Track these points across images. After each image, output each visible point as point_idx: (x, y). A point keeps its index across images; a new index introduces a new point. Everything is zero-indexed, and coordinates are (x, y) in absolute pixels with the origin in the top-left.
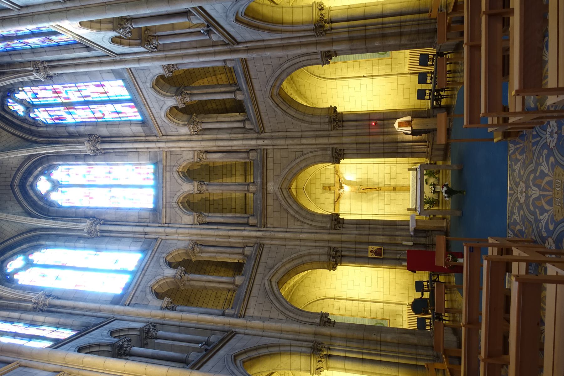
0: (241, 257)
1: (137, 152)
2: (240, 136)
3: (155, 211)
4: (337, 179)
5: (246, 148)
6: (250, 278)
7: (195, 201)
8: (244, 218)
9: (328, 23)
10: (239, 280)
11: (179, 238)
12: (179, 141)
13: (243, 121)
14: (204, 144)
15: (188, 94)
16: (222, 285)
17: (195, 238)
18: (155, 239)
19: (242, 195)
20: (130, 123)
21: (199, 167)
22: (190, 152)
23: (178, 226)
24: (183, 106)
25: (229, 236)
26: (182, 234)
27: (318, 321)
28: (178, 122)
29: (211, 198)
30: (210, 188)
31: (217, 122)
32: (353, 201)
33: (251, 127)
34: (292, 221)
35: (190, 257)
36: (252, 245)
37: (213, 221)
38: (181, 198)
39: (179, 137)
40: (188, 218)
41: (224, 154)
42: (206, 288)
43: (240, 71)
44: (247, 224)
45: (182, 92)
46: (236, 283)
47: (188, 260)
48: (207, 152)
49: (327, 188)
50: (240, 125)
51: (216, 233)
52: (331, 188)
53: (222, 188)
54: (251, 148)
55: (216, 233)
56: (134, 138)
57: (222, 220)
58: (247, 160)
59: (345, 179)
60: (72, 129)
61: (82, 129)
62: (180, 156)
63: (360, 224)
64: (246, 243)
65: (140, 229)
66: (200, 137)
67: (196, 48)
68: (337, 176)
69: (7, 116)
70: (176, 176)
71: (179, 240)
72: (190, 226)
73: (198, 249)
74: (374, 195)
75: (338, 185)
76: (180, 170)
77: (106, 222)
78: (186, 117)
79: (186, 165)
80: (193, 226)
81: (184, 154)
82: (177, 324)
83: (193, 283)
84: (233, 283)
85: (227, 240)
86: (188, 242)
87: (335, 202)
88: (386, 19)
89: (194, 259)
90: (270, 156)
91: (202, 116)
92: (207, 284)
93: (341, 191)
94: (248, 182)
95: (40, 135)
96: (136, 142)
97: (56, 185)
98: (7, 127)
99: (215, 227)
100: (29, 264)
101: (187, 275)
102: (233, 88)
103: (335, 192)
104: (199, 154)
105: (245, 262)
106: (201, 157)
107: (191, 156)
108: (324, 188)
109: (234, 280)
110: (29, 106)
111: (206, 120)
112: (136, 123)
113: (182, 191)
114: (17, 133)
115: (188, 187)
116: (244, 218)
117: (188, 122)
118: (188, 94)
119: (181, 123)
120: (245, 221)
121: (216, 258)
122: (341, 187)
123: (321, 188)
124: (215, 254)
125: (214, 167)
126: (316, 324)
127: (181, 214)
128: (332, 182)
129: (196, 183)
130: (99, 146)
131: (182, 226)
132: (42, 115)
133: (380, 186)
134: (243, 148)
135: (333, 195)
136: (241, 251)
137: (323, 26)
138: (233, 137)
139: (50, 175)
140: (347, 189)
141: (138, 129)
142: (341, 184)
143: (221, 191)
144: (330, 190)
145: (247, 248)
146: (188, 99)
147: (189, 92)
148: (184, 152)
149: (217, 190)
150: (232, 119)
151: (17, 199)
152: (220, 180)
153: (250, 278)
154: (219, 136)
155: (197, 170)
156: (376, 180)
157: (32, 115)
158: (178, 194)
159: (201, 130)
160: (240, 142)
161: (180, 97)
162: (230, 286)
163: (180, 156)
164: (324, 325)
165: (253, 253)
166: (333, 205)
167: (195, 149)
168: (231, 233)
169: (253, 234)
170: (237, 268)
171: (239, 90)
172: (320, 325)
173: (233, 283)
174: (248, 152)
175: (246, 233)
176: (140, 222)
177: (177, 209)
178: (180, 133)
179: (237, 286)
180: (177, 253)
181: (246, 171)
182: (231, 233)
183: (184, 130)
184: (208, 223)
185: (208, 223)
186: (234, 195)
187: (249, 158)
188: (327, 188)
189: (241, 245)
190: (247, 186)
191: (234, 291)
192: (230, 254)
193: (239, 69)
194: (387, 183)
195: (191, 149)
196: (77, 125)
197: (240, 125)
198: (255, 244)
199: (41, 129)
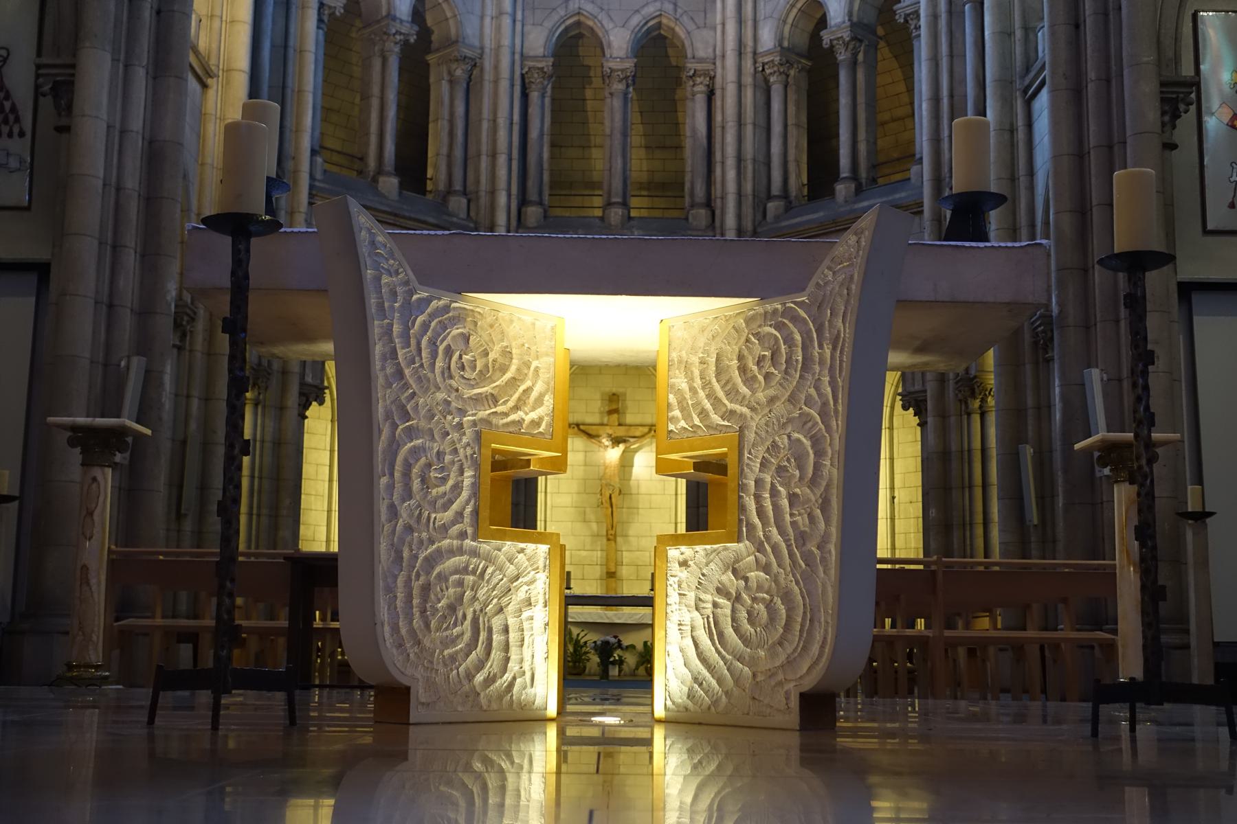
0: (442, 187)
2: (748, 187)
4: (638, 432)
5: (719, 202)
6: (396, 215)
7: (581, 51)
8: (540, 193)
9: (981, 407)
10: (389, 184)
11: (487, 20)
12: (740, 22)
13: (785, 195)
14: (731, 89)
15: (855, 55)
16: (373, 139)
17: (488, 64)
19: (596, 177)
21: (674, 62)
22: (710, 50)
23: (519, 16)
24: (826, 43)
25: (493, 156)
26: (499, 29)
27: (309, 379)
28: (790, 20)
29: (589, 93)
30: (617, 103)
31: (786, 126)
33: (770, 215)
35: (438, 50)
36: (472, 214)
37: (530, 110)
38: (590, 23)
39: (750, 23)
40: (538, 41)
41: (705, 141)
42: (366, 97)
43: (897, 196)
44: (523, 202)
45: (861, 41)
46: (382, 179)
47: (431, 42)
48: (710, 94)
50: (776, 187)
51: (502, 121)
52: (615, 416)
53: (618, 136)
54: (718, 212)
55: (502, 121)
57: (534, 134)
58: (687, 200)
59: (636, 451)
62: (701, 22)
64: (478, 198)
66: (748, 79)
67: (951, 96)
68: (646, 430)
70: (651, 9)
71: (482, 18)
72: (518, 48)
74: (594, 526)
75: (621, 432)
76: (664, 21)
78: (802, 41)
79: (679, 37)
80: (517, 57)
81: (706, 33)
82: (291, 43)
83: (377, 64)
84: (380, 171)
85: (484, 148)
86: (477, 43)
87: (578, 425)
88: (979, 531)
89: (431, 58)
91: (804, 85)
92: (375, 102)
93: (606, 442)
94: (634, 202)
99: (516, 118)
101: (397, 49)
102: (863, 173)
103: (602, 425)
104: (706, 74)
105: (429, 197)
106: (699, 80)
107: (701, 53)
109: (388, 174)
111: (792, 97)
113: (609, 25)
116: (540, 193)
117: (788, 49)
118: (855, 55)
119: (787, 28)
120: (533, 195)
121: (437, 120)
122: (616, 441)
123: (614, 390)
124: (446, 116)
125: (674, 101)
126: (303, 375)
127: (548, 24)
128: (629, 419)
129: (629, 64)
131: (519, 26)
133: (619, 539)
134: (719, 193)
135: (595, 419)
136: (458, 186)
137: (973, 396)
138: (745, 167)
140: (613, 455)
142: (624, 441)
143: (608, 131)
144: (610, 412)
145: (465, 201)
146: (842, 56)
147: (861, 57)
148: (712, 33)
149: (612, 120)
150: (792, 167)
152: (639, 129)
153: (396, 215)
154: (749, 130)
155: (667, 56)
156: (633, 530)
158: (602, 16)
159: (766, 81)
160: (731, 187)
161: (847, 35)
162: (372, 163)
163: (701, 22)
164: (301, 394)
165: (455, 219)
167: (718, 63)
168: (502, 160)
171: (859, 190)
172: (303, 384)
173: (380, 171)
174: (709, 204)
175: (502, 199)
177: (562, 13)
178: (761, 24)
179: (375, 180)
180: (449, 14)
181: (663, 186)
182: (502, 160)
183: (767, 38)
184: (525, 96)
185: (525, 96)
186: (596, 153)
187: (692, 206)
189: (470, 187)
190: (619, 200)
191: (360, 172)
192: (449, 156)
193: (903, 194)
194: (626, 557)
195: (718, 52)
197: (776, 187)
198: (476, 223)
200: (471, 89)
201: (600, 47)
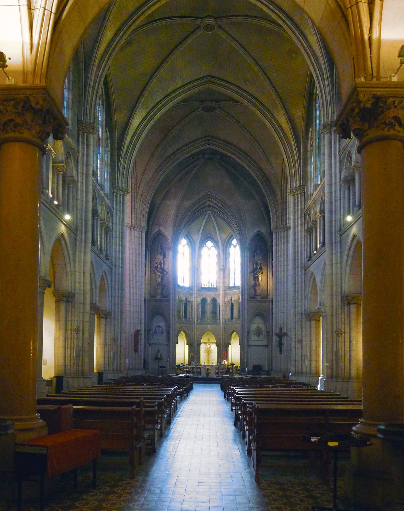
0: (189, 318)
1: (220, 283)
3: (203, 289)
10: (184, 319)
14: (222, 306)
18: (193, 290)
20: (229, 282)
32: (204, 348)
40: (199, 300)
44: (198, 319)
49: (209, 340)
56: (224, 283)
60: (227, 260)
61: (227, 264)
65: (196, 286)
69: (232, 238)
73: (191, 304)
77: (197, 271)
95: (226, 247)
98: (228, 237)
100: (184, 246)
108: (209, 339)
112: (229, 284)
115: (209, 300)
130: (222, 270)
135: (206, 342)
139: (213, 246)
157: (232, 246)
166: (204, 342)
169: (196, 322)
170: (185, 317)
174: (220, 319)
175: (196, 320)
176: (199, 283)
188: (209, 340)
196: (229, 262)
199: (228, 248)
200: (192, 306)
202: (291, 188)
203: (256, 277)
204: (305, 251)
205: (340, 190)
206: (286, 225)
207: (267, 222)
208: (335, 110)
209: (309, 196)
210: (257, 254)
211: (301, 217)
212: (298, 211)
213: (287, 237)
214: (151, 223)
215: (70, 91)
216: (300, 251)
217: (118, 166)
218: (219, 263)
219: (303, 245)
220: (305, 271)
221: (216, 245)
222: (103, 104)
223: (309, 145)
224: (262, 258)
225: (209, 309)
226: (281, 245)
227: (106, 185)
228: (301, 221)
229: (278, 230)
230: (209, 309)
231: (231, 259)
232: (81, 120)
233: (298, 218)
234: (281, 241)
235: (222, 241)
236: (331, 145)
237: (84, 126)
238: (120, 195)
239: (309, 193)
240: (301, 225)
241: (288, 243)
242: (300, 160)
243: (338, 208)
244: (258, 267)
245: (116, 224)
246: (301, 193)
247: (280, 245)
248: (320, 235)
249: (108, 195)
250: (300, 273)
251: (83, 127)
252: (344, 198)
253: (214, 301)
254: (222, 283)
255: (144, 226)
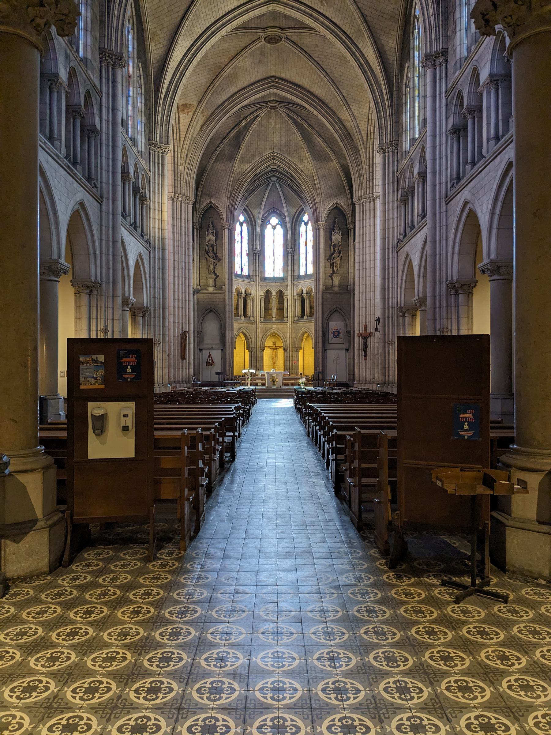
1: (288, 271)
10: (243, 317)
34: (262, 334)
40: (262, 293)
60: (297, 242)
61: (297, 247)
63: (262, 357)
73: (251, 299)
90: (285, 326)
96: (292, 271)
97: (274, 228)
110: (306, 224)
114: (296, 215)
115: (274, 293)
132: (303, 228)
141: (296, 274)
146: (305, 298)
151: (268, 211)
157: (303, 223)
170: (245, 315)
183: (295, 294)
201: (271, 293)
202: (380, 144)
203: (333, 263)
204: (398, 227)
205: (447, 143)
206: (372, 193)
207: (348, 192)
208: (441, 36)
209: (404, 154)
210: (335, 233)
211: (393, 183)
212: (389, 174)
213: (374, 210)
214: (200, 193)
215: (88, 7)
216: (391, 226)
217: (155, 115)
218: (285, 245)
219: (396, 219)
220: (397, 252)
221: (283, 223)
222: (133, 29)
223: (404, 86)
224: (340, 237)
225: (274, 305)
226: (366, 219)
227: (140, 140)
228: (393, 186)
229: (361, 202)
230: (274, 305)
231: (302, 241)
232: (104, 48)
233: (389, 184)
234: (366, 215)
235: (289, 217)
236: (435, 82)
237: (109, 56)
238: (159, 152)
239: (404, 150)
240: (393, 192)
241: (374, 217)
242: (392, 106)
243: (444, 168)
244: (336, 249)
245: (154, 192)
246: (393, 151)
247: (364, 221)
248: (418, 205)
249: (143, 153)
250: (391, 256)
251: (107, 58)
252: (452, 153)
253: (281, 294)
254: (290, 272)
255: (191, 196)
